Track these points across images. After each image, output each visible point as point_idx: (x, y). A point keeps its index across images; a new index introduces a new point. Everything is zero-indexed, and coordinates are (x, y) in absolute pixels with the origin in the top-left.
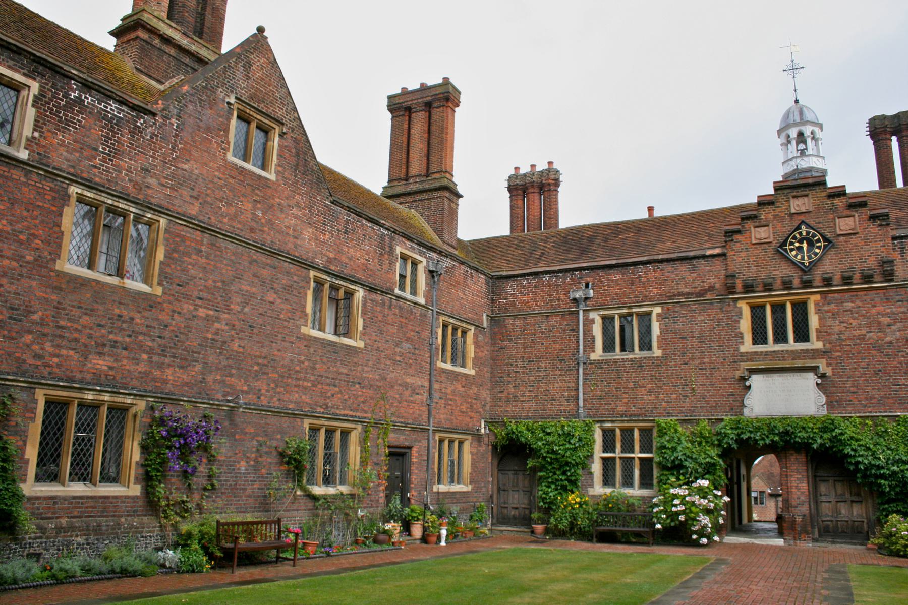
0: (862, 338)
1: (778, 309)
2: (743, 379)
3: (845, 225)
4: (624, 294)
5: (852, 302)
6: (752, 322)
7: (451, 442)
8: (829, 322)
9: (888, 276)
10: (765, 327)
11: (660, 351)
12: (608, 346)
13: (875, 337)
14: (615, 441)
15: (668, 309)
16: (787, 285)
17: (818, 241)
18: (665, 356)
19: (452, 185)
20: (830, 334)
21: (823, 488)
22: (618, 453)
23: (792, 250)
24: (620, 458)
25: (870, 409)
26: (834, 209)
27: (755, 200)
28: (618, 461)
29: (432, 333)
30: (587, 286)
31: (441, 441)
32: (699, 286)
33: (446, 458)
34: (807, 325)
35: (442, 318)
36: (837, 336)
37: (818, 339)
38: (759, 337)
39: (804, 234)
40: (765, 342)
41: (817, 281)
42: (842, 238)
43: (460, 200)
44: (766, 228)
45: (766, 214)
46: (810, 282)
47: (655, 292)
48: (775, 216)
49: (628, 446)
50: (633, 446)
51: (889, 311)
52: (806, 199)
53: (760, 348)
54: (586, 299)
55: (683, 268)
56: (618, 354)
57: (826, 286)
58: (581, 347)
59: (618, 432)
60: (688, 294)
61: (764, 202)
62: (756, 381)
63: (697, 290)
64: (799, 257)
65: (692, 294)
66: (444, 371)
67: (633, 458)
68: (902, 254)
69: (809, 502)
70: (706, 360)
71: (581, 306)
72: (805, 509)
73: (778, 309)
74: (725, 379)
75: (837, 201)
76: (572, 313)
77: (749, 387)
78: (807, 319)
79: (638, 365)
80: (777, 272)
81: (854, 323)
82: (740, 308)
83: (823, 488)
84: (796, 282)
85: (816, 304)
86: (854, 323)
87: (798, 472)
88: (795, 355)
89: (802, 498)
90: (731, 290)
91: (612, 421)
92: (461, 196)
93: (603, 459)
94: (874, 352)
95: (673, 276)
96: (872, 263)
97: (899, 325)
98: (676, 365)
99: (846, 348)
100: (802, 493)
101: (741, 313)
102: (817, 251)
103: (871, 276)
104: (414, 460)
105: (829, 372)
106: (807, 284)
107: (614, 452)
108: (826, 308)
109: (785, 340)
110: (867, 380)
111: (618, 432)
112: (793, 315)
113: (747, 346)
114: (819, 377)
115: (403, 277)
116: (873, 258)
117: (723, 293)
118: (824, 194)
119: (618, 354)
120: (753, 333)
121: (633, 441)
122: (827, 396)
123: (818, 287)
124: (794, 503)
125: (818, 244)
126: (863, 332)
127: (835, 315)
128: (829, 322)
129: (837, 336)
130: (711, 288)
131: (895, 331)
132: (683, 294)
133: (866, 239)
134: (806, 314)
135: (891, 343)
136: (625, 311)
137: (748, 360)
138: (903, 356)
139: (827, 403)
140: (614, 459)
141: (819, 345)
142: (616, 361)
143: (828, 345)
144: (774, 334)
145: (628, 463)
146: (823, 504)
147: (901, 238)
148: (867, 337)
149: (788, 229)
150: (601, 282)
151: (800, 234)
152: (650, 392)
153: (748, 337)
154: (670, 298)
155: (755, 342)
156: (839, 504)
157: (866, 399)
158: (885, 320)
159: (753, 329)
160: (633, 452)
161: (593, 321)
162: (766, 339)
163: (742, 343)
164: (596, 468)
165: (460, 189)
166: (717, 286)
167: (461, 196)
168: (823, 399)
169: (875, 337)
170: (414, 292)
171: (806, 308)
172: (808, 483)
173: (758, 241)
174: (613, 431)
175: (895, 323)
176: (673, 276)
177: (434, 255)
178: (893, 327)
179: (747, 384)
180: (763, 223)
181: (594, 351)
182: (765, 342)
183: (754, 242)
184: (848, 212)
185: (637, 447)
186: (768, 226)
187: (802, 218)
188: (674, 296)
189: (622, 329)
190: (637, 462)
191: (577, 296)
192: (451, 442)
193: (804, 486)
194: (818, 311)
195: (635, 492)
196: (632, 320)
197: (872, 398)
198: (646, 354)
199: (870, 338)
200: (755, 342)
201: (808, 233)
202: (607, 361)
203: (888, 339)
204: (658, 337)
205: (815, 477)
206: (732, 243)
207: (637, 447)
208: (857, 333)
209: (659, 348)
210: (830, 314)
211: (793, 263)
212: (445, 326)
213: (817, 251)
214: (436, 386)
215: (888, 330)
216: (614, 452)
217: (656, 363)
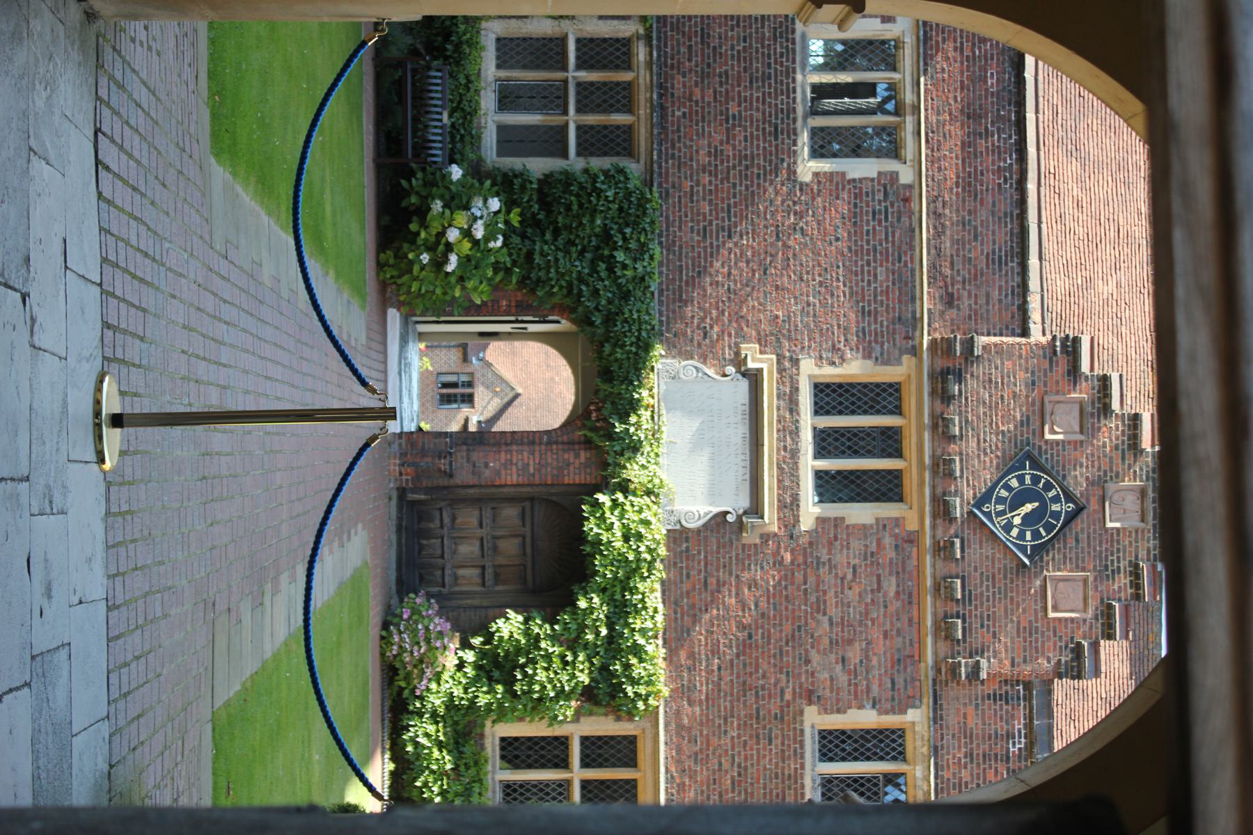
1: (890, 442)
5: (898, 593)
6: (865, 386)
8: (856, 545)
10: (853, 413)
11: (807, 178)
14: (604, 67)
17: (1036, 535)
20: (830, 544)
21: (510, 513)
22: (575, 75)
23: (1021, 479)
24: (566, 81)
28: (559, 75)
34: (852, 500)
38: (831, 397)
39: (1055, 507)
40: (819, 410)
44: (1077, 429)
49: (590, 97)
50: (592, 111)
51: (875, 662)
52: (1137, 516)
64: (1004, 493)
67: (565, 112)
68: (995, 697)
69: (481, 486)
72: (463, 476)
73: (890, 442)
78: (865, 500)
81: (852, 595)
82: (898, 362)
83: (510, 513)
85: (897, 522)
86: (852, 595)
87: (540, 467)
89: (487, 473)
91: (649, 64)
93: (563, 40)
94: (788, 627)
95: (983, 214)
97: (843, 679)
99: (799, 576)
100: (498, 473)
101: (887, 363)
107: (579, 67)
108: (888, 541)
109: (822, 450)
111: (626, 76)
112: (877, 472)
113: (810, 370)
114: (739, 517)
120: (840, 386)
121: (605, 111)
122: (699, 531)
124: (475, 456)
125: (1028, 535)
126: (833, 611)
127: (871, 557)
128: (856, 545)
129: (825, 558)
131: (832, 670)
134: (877, 500)
135: (808, 662)
137: (781, 370)
138: (777, 682)
139: (684, 530)
140: (565, 68)
144: (836, 430)
145: (553, 98)
146: (476, 513)
147: (1028, 698)
148: (820, 617)
151: (1056, 499)
152: (715, 153)
153: (830, 373)
156: (478, 543)
158: (854, 654)
159: (852, 385)
162: (828, 413)
171: (890, 500)
173: (1048, 408)
175: (849, 673)
176: (983, 214)
178: (839, 668)
180: (1089, 422)
183: (1046, 399)
185: (591, 119)
186: (1081, 432)
189: (868, 89)
190: (556, 120)
193: (512, 477)
194: (882, 525)
195: (490, 118)
199: (818, 622)
201: (1056, 515)
203: (814, 655)
204: (843, 174)
205: (532, 499)
207: (591, 119)
209: (816, 174)
210: (874, 547)
215: (833, 657)
216: (579, 67)
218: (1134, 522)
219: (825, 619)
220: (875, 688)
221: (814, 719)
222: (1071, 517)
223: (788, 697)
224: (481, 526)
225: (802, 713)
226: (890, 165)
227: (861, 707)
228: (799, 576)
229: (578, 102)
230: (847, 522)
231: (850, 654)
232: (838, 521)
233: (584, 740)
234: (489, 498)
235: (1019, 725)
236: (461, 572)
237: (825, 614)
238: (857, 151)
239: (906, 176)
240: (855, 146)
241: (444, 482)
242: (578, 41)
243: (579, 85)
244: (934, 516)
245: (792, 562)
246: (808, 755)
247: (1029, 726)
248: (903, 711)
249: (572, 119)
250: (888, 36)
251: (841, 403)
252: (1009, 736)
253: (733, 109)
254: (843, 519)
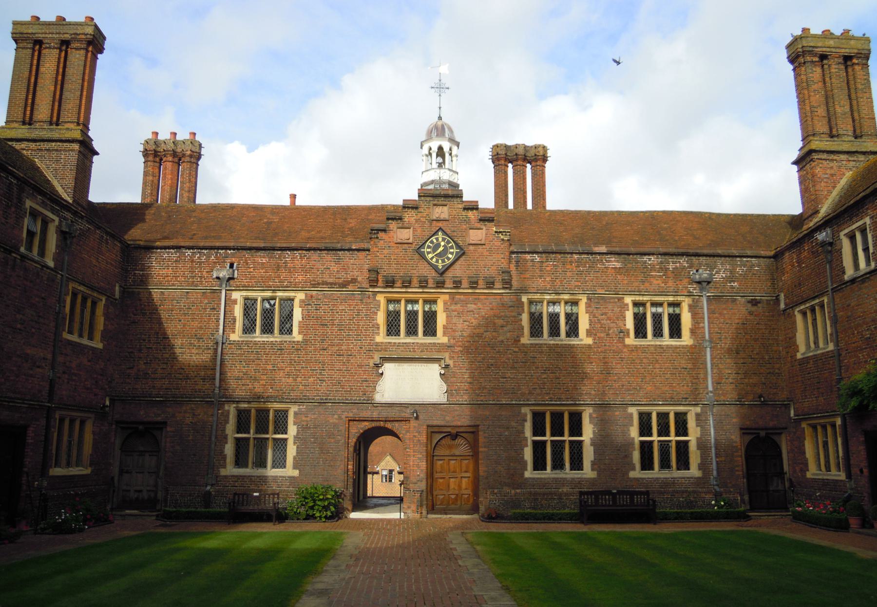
2: (377, 366)
3: (476, 235)
4: (269, 278)
7: (72, 421)
8: (454, 320)
9: (507, 284)
12: (249, 329)
15: (312, 296)
16: (423, 283)
17: (452, 247)
18: (305, 341)
19: (87, 140)
20: (454, 331)
24: (255, 438)
25: (482, 398)
26: (467, 221)
27: (401, 203)
28: (252, 441)
29: (61, 301)
30: (232, 266)
31: (62, 420)
32: (343, 277)
33: (65, 438)
35: (71, 285)
37: (444, 334)
40: (398, 334)
41: (449, 284)
42: (471, 248)
43: (95, 158)
45: (409, 217)
46: (443, 283)
47: (300, 278)
48: (417, 221)
53: (393, 340)
54: (230, 279)
55: (328, 257)
56: (258, 336)
57: (455, 288)
58: (221, 327)
59: (253, 411)
60: (331, 284)
61: (409, 206)
62: (389, 368)
63: (341, 281)
65: (335, 284)
66: (70, 343)
67: (268, 439)
71: (224, 286)
74: (360, 366)
75: (470, 214)
76: (214, 291)
77: (382, 374)
79: (280, 348)
80: (415, 272)
82: (379, 301)
84: (431, 283)
85: (445, 303)
90: (373, 283)
92: (97, 154)
94: (488, 349)
96: (492, 272)
97: (509, 327)
98: (315, 350)
100: (422, 470)
101: (379, 306)
102: (450, 256)
103: (493, 283)
104: (30, 441)
105: (451, 363)
106: (440, 284)
107: (249, 433)
108: (453, 307)
111: (253, 411)
113: (381, 337)
115: (31, 234)
116: (494, 268)
117: (363, 286)
118: (461, 206)
119: (258, 336)
121: (268, 422)
123: (448, 288)
125: (452, 250)
126: (482, 331)
128: (454, 320)
129: (460, 333)
130: (354, 281)
132: (327, 283)
133: (490, 250)
135: (502, 341)
136: (268, 294)
140: (249, 439)
141: (445, 340)
142: (256, 343)
149: (427, 233)
150: (247, 264)
153: (383, 329)
154: (314, 286)
155: (389, 333)
157: (479, 389)
160: (268, 433)
161: (235, 302)
163: (378, 334)
164: (229, 449)
165: (96, 145)
166: (359, 279)
167: (97, 154)
168: (445, 388)
170: (42, 252)
173: (399, 241)
174: (248, 411)
177: (68, 215)
179: (380, 371)
181: (234, 332)
182: (398, 334)
184: (479, 225)
187: (440, 224)
188: (319, 284)
191: (221, 276)
192: (72, 421)
193: (423, 465)
196: (274, 304)
197: (484, 388)
198: (286, 338)
200: (389, 333)
202: (247, 343)
203: (501, 338)
206: (376, 240)
209: (299, 333)
211: (429, 263)
212: (75, 295)
213: (450, 256)
214: (60, 359)
216: (249, 433)
217: (297, 347)
218: (445, 208)
220: (513, 314)
221: (526, 340)
222: (445, 233)
223: (517, 350)
225: (523, 344)
226: (296, 303)
227: (521, 320)
229: (264, 433)
232: (445, 327)
233: (535, 435)
235: (528, 257)
238: (290, 316)
239: (300, 296)
240: (288, 318)
241: (425, 493)
242: (238, 433)
243: (256, 433)
244: (443, 287)
246: (541, 342)
247: (529, 253)
248: (523, 303)
249: (271, 436)
250: (242, 302)
252: (532, 261)
253: (269, 367)
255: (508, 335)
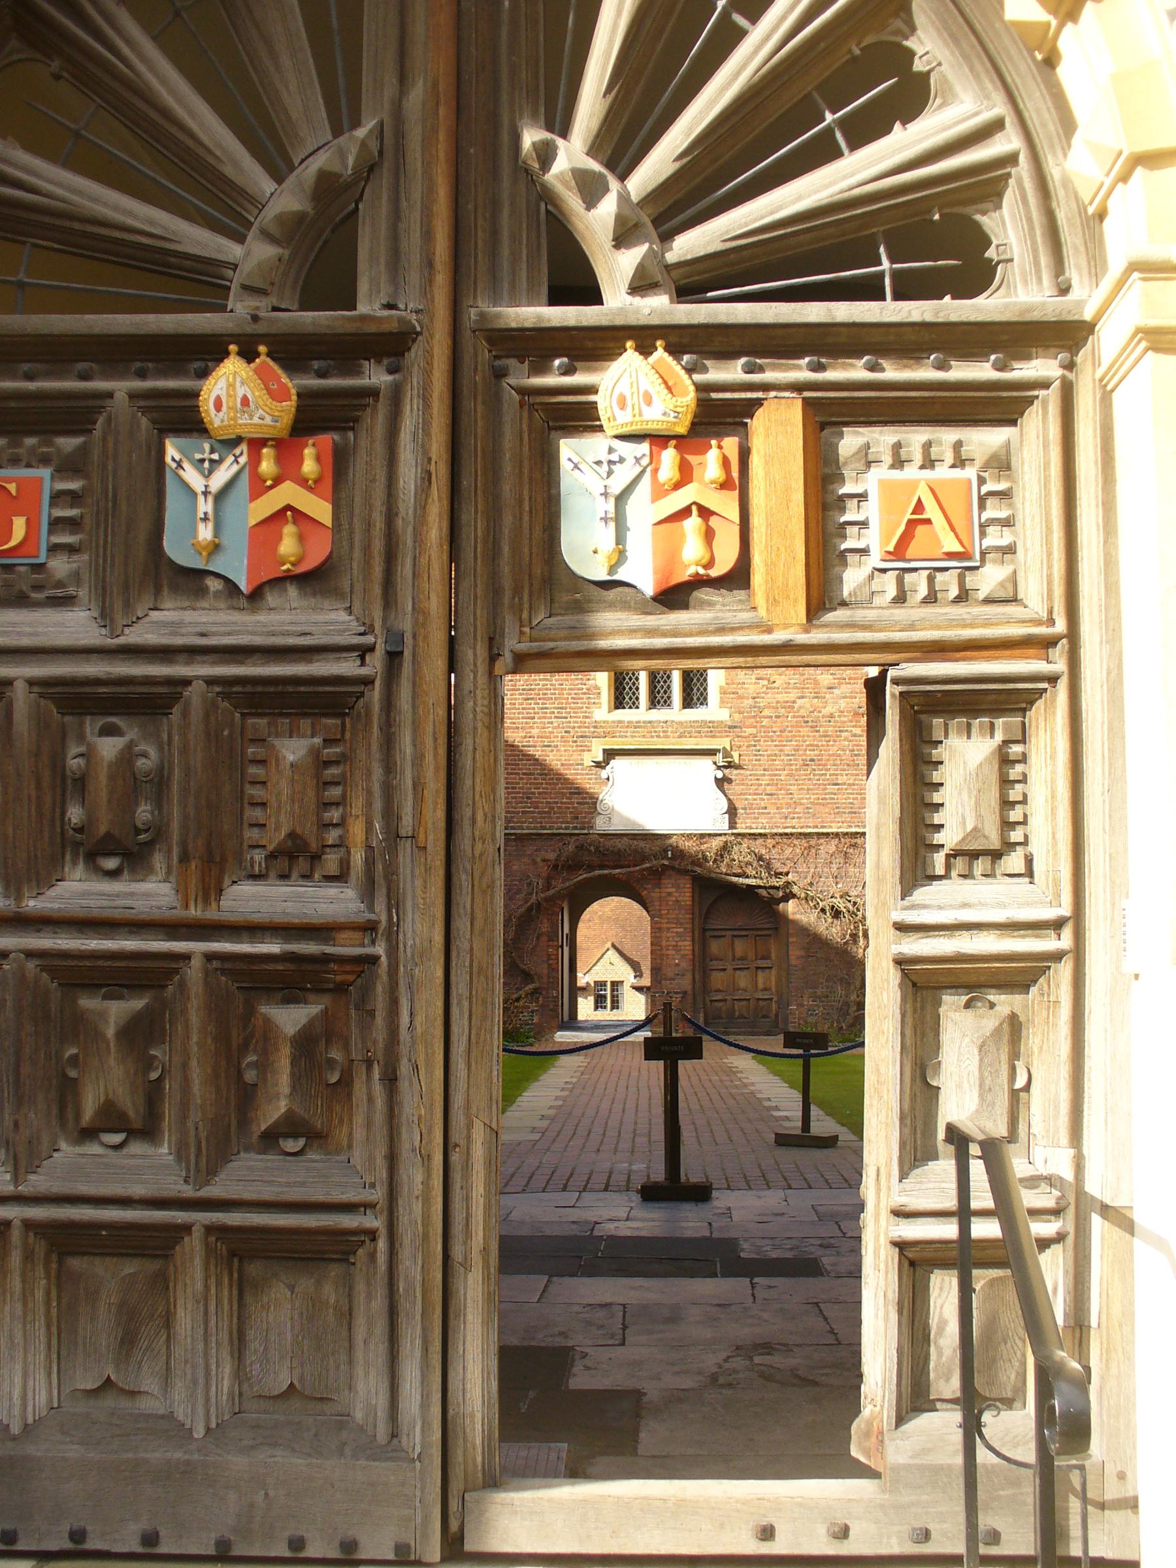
0: (789, 706)
13: (808, 706)
20: (740, 698)
21: (715, 947)
36: (751, 701)
37: (723, 703)
69: (693, 970)
70: (535, 732)
72: (686, 983)
83: (715, 947)
87: (679, 923)
88: (686, 729)
89: (684, 965)
94: (805, 731)
99: (765, 722)
100: (684, 956)
110: (791, 775)
126: (792, 696)
129: (751, 701)
135: (832, 716)
143: (737, 716)
156: (738, 972)
157: (789, 805)
169: (808, 706)
172: (693, 940)
175: (840, 684)
178: (836, 691)
193: (686, 945)
205: (705, 930)
208: (780, 697)
219: (799, 701)
224: (724, 970)
228: (765, 722)
230: (723, 684)
231: (826, 683)
232: (723, 692)
234: (702, 963)
236: (760, 986)
237: (794, 702)
241: (690, 998)
245: (755, 727)
251: (630, 689)
254: (721, 688)
255: (843, 704)
